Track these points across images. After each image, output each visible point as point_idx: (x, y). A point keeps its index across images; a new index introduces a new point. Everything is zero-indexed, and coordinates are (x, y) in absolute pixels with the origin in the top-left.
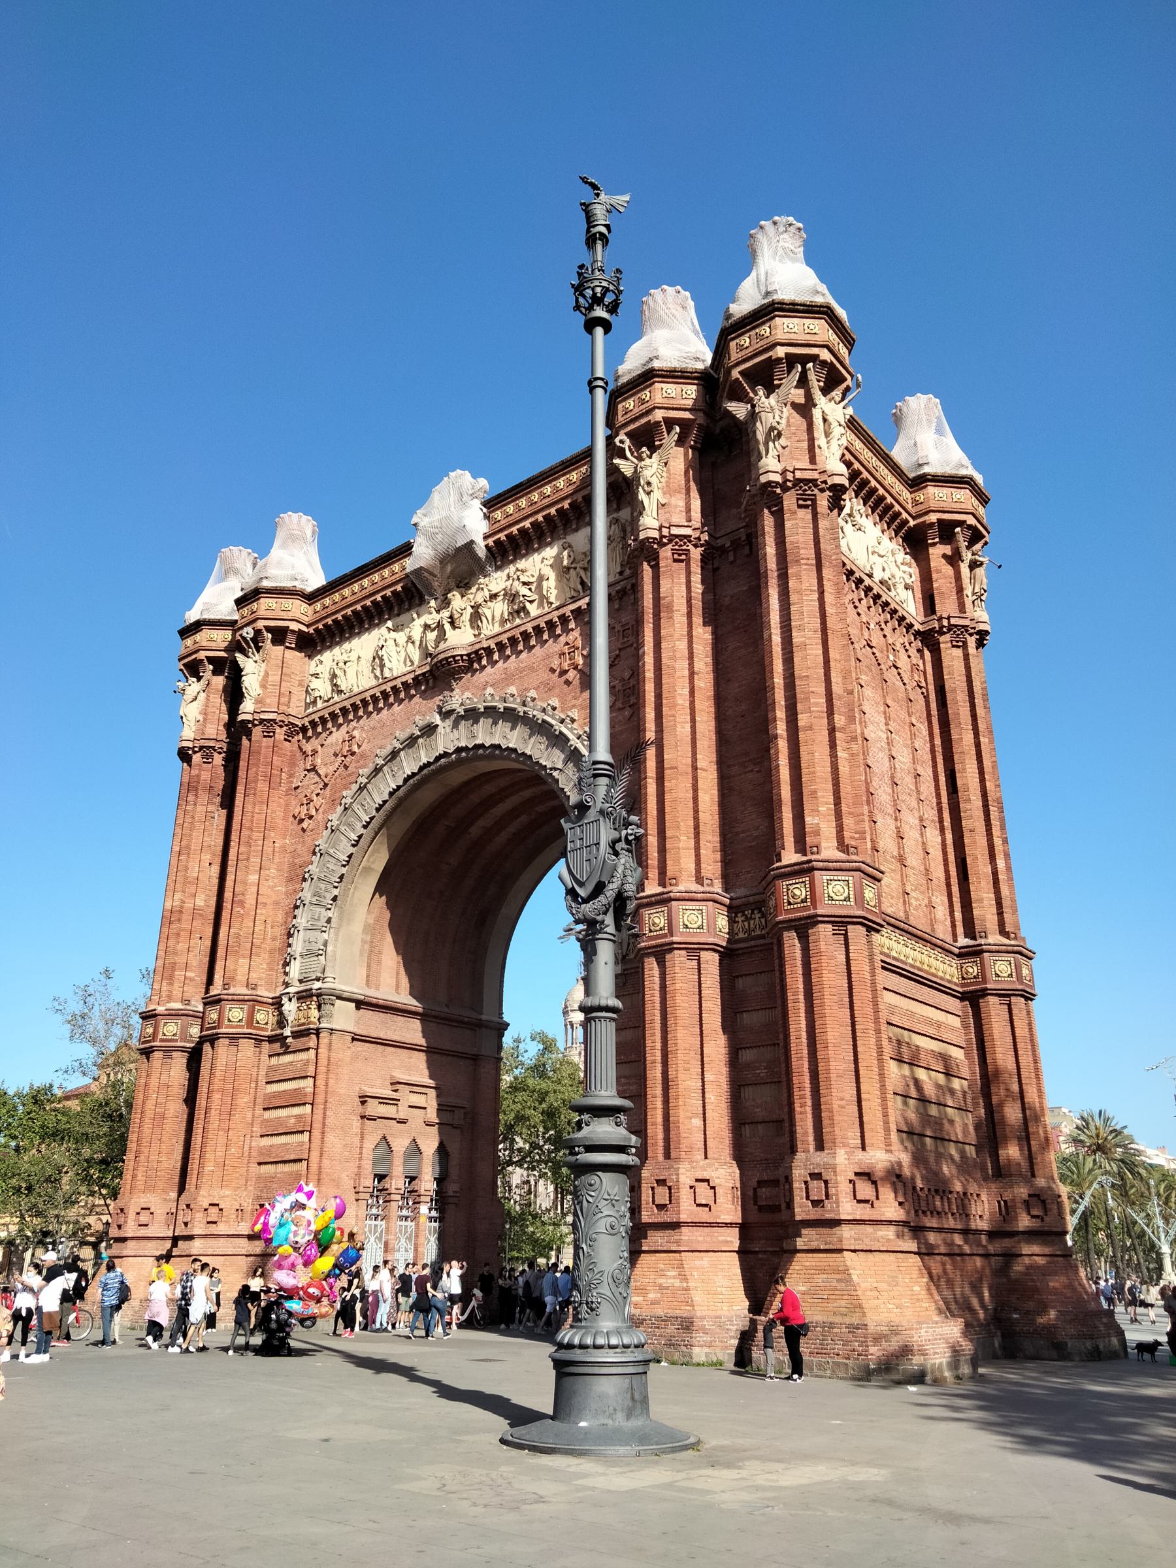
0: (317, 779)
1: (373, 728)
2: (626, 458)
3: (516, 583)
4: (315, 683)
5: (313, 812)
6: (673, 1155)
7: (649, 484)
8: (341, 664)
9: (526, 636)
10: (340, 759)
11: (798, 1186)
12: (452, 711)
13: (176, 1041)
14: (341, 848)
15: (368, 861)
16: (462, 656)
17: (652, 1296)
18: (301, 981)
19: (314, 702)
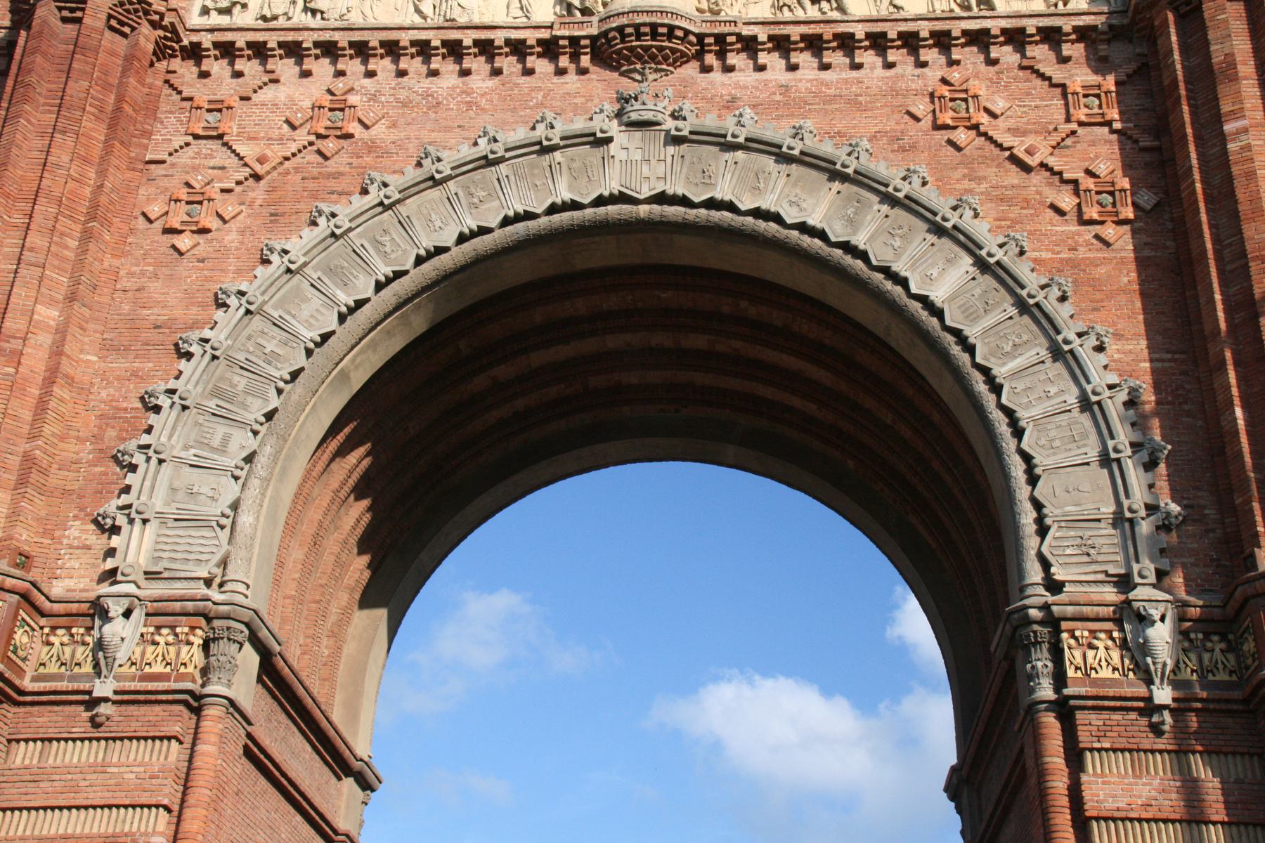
0: (222, 157)
1: (405, 105)
10: (303, 136)
14: (305, 314)
15: (353, 360)
16: (687, 32)
18: (150, 575)
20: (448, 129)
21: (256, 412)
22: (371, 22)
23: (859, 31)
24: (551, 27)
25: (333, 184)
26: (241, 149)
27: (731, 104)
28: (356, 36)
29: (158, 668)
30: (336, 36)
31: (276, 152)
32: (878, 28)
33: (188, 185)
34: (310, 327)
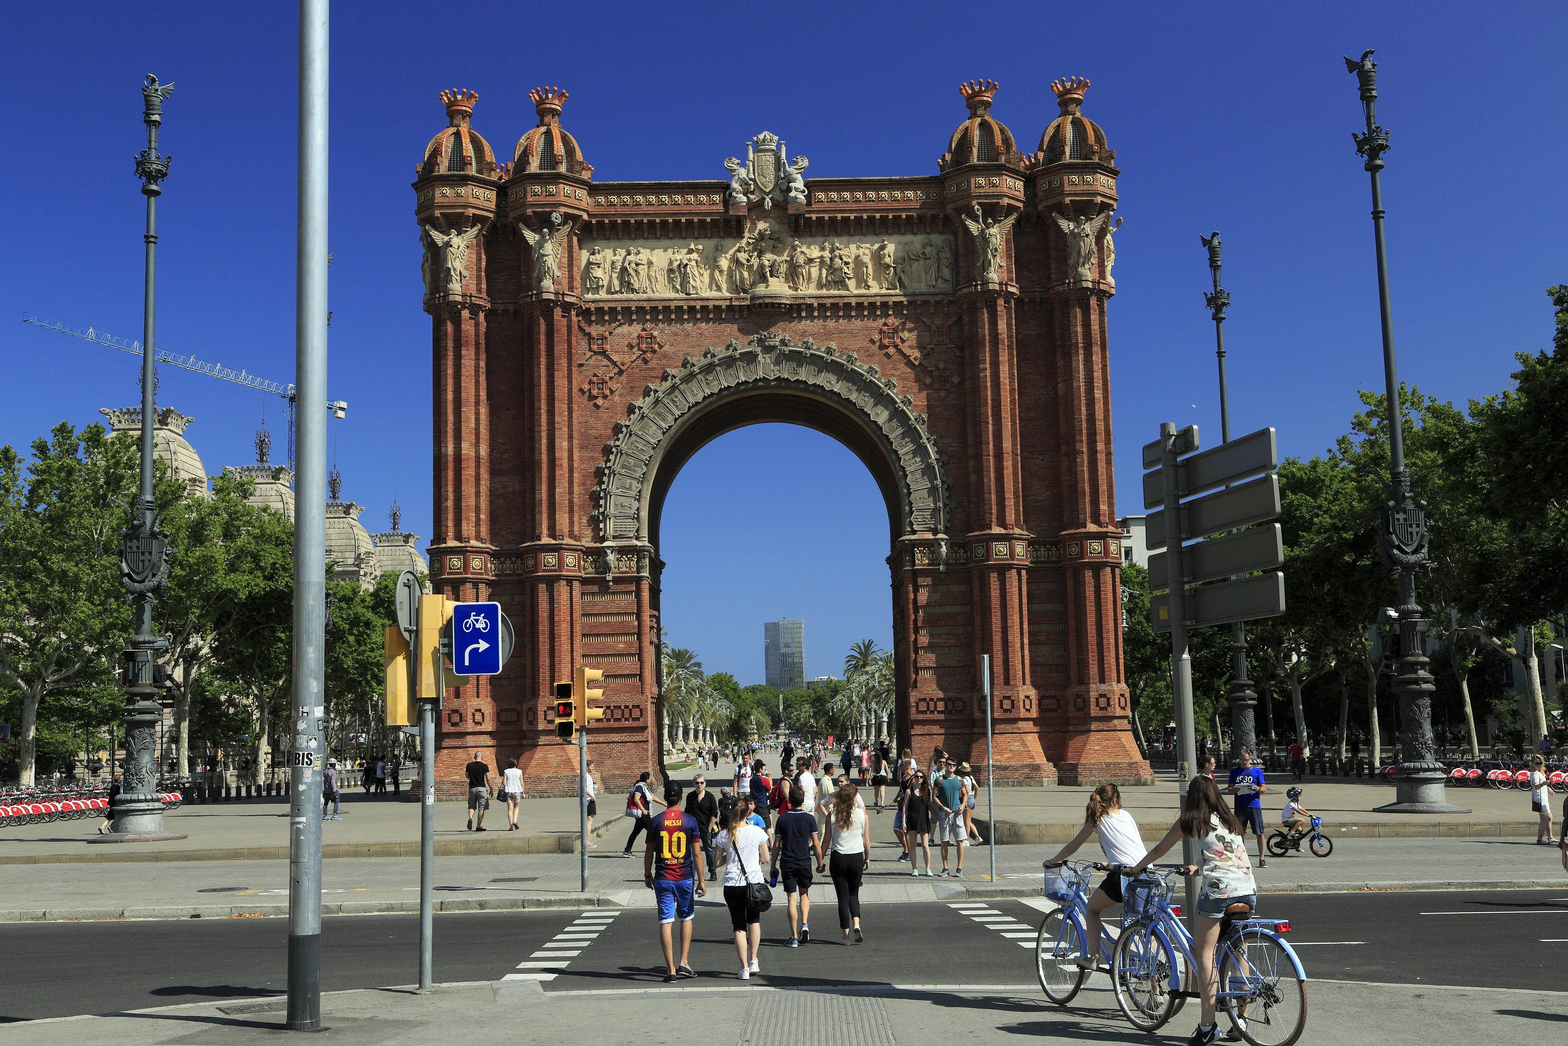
0: (606, 362)
1: (675, 335)
2: (977, 221)
3: (837, 260)
4: (598, 273)
5: (607, 392)
6: (1012, 683)
7: (996, 250)
8: (633, 265)
9: (847, 306)
11: (1093, 700)
12: (775, 347)
13: (482, 574)
17: (1006, 755)
18: (615, 537)
19: (597, 290)
20: (693, 347)
21: (639, 474)
22: (657, 295)
23: (853, 301)
24: (731, 299)
25: (652, 373)
26: (615, 358)
27: (804, 333)
28: (653, 304)
29: (624, 569)
30: (645, 304)
31: (627, 359)
32: (860, 300)
33: (595, 375)
34: (653, 438)
